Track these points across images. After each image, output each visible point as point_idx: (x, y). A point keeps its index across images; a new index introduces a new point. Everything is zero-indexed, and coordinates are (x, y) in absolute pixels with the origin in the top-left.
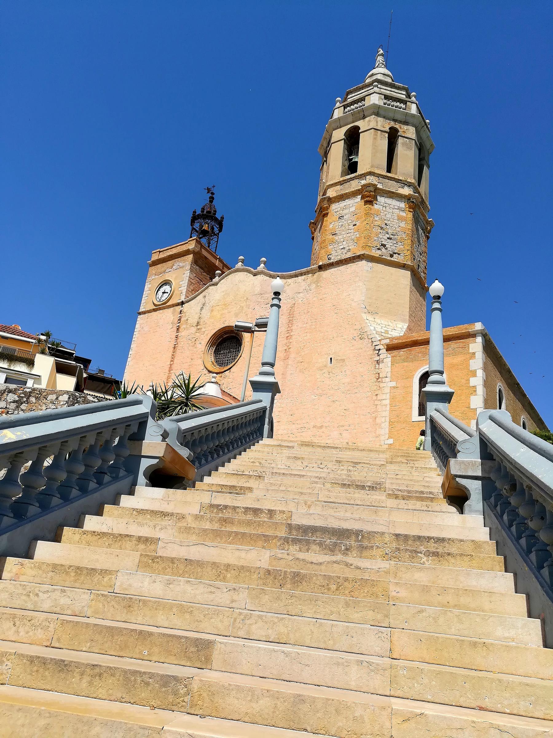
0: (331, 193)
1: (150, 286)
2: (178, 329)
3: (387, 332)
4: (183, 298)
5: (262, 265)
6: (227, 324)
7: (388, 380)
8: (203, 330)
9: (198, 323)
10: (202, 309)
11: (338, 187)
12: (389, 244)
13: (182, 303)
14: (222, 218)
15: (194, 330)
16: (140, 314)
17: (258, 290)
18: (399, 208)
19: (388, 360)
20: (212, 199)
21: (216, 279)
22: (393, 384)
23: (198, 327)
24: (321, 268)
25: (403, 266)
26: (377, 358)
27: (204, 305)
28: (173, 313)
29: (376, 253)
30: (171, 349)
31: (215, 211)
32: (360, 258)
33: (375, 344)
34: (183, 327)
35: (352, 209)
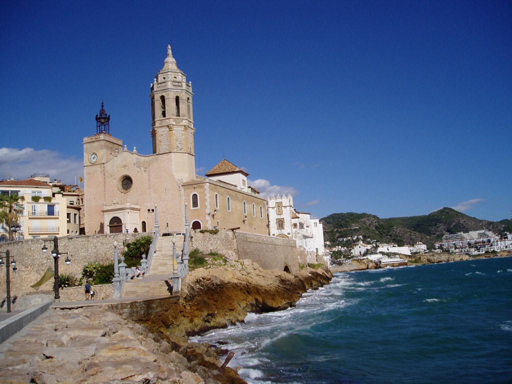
3: (182, 179)
5: (135, 150)
6: (123, 174)
12: (179, 145)
14: (109, 116)
17: (135, 161)
18: (182, 131)
20: (103, 106)
24: (157, 155)
28: (101, 167)
29: (175, 150)
31: (106, 115)
35: (166, 132)
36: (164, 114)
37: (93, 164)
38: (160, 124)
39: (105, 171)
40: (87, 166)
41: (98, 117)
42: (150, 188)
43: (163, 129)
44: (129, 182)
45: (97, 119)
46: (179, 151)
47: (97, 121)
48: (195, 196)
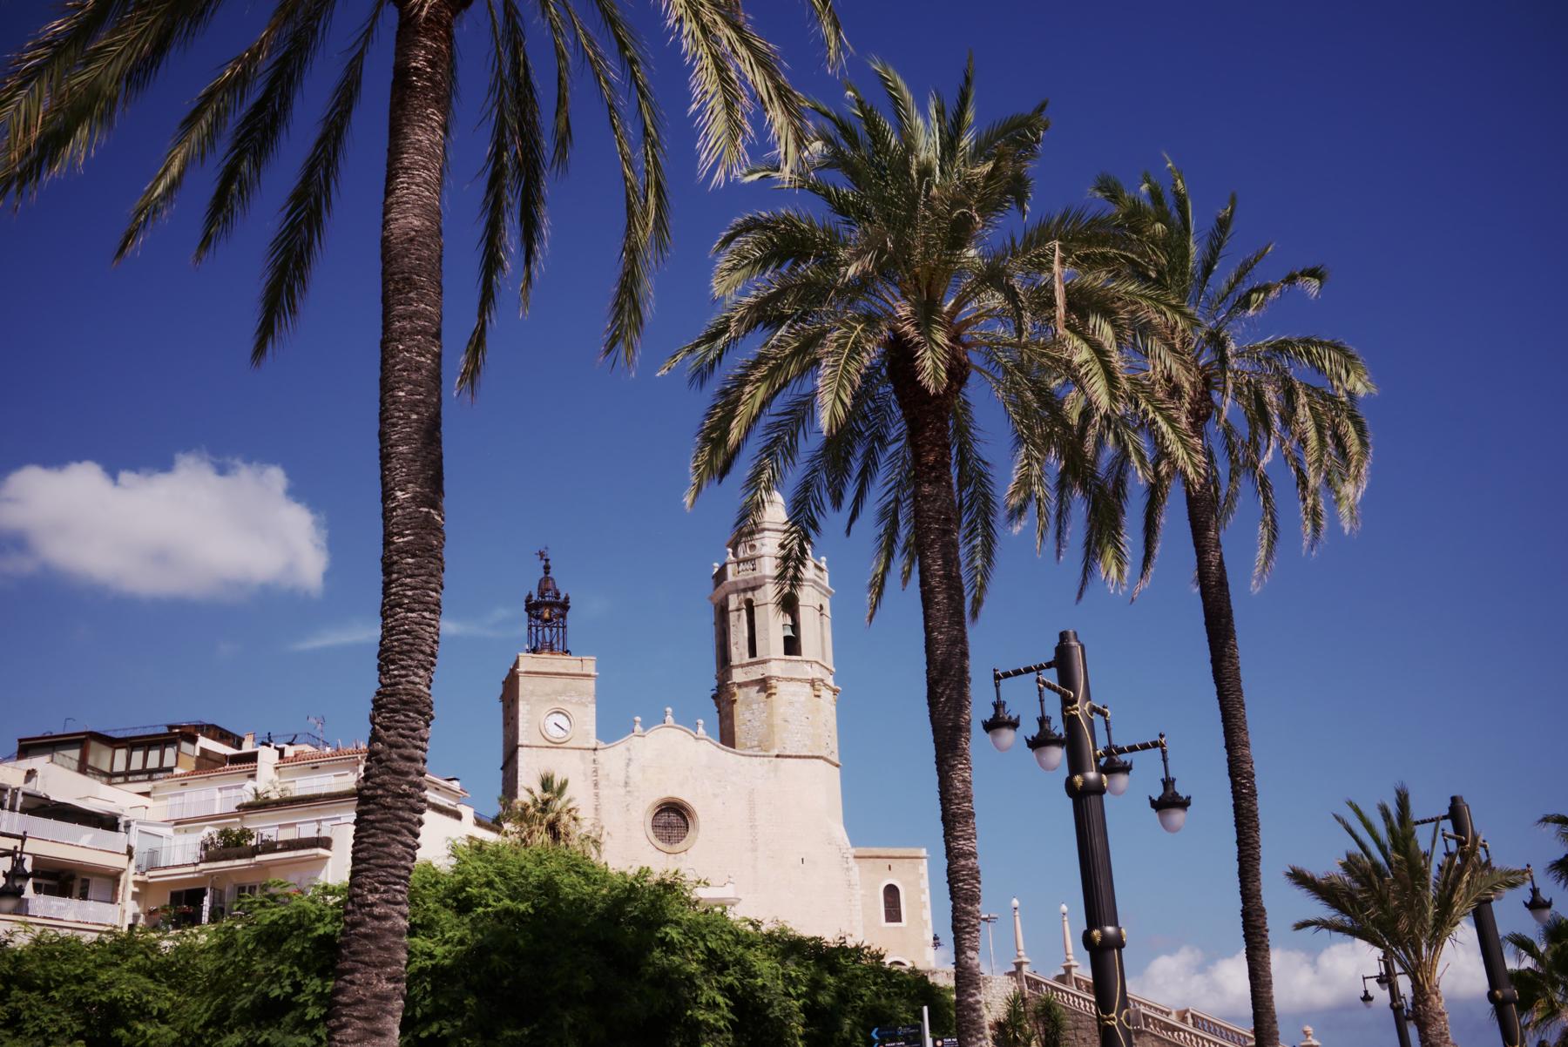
0: (774, 669)
1: (528, 707)
2: (596, 785)
4: (593, 742)
5: (701, 730)
7: (858, 887)
8: (636, 794)
9: (626, 783)
10: (628, 765)
11: (783, 662)
12: (829, 740)
13: (595, 749)
15: (622, 791)
16: (522, 746)
19: (856, 869)
20: (547, 569)
21: (638, 728)
22: (862, 892)
23: (628, 789)
24: (778, 756)
25: (837, 766)
26: (846, 866)
27: (630, 760)
30: (593, 811)
31: (567, 599)
32: (818, 757)
33: (843, 851)
34: (602, 783)
36: (792, 646)
37: (556, 745)
38: (782, 670)
39: (600, 772)
40: (527, 746)
41: (535, 598)
42: (754, 850)
43: (793, 687)
44: (674, 818)
45: (532, 608)
46: (830, 758)
47: (530, 615)
48: (892, 893)
